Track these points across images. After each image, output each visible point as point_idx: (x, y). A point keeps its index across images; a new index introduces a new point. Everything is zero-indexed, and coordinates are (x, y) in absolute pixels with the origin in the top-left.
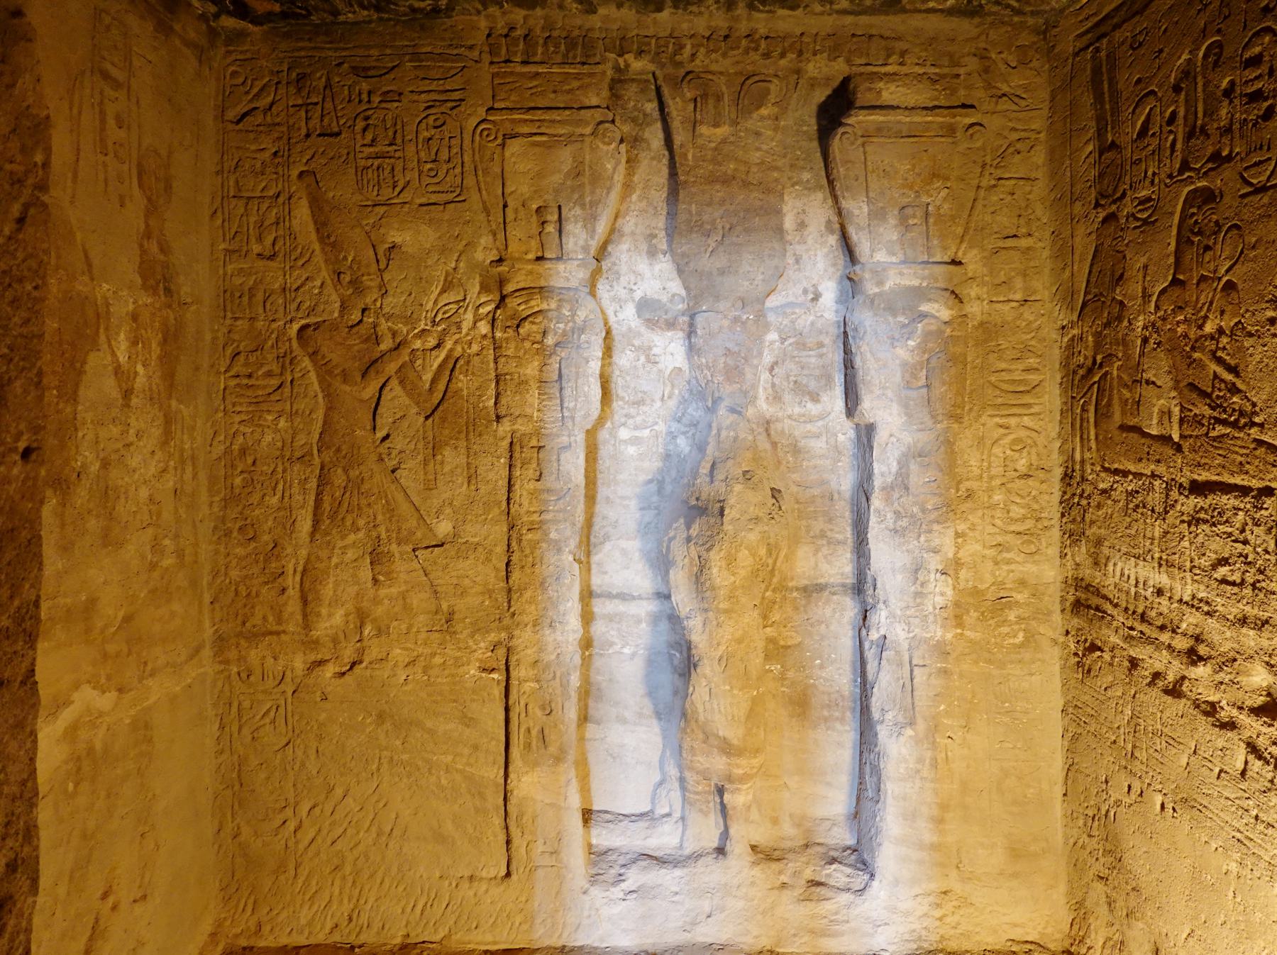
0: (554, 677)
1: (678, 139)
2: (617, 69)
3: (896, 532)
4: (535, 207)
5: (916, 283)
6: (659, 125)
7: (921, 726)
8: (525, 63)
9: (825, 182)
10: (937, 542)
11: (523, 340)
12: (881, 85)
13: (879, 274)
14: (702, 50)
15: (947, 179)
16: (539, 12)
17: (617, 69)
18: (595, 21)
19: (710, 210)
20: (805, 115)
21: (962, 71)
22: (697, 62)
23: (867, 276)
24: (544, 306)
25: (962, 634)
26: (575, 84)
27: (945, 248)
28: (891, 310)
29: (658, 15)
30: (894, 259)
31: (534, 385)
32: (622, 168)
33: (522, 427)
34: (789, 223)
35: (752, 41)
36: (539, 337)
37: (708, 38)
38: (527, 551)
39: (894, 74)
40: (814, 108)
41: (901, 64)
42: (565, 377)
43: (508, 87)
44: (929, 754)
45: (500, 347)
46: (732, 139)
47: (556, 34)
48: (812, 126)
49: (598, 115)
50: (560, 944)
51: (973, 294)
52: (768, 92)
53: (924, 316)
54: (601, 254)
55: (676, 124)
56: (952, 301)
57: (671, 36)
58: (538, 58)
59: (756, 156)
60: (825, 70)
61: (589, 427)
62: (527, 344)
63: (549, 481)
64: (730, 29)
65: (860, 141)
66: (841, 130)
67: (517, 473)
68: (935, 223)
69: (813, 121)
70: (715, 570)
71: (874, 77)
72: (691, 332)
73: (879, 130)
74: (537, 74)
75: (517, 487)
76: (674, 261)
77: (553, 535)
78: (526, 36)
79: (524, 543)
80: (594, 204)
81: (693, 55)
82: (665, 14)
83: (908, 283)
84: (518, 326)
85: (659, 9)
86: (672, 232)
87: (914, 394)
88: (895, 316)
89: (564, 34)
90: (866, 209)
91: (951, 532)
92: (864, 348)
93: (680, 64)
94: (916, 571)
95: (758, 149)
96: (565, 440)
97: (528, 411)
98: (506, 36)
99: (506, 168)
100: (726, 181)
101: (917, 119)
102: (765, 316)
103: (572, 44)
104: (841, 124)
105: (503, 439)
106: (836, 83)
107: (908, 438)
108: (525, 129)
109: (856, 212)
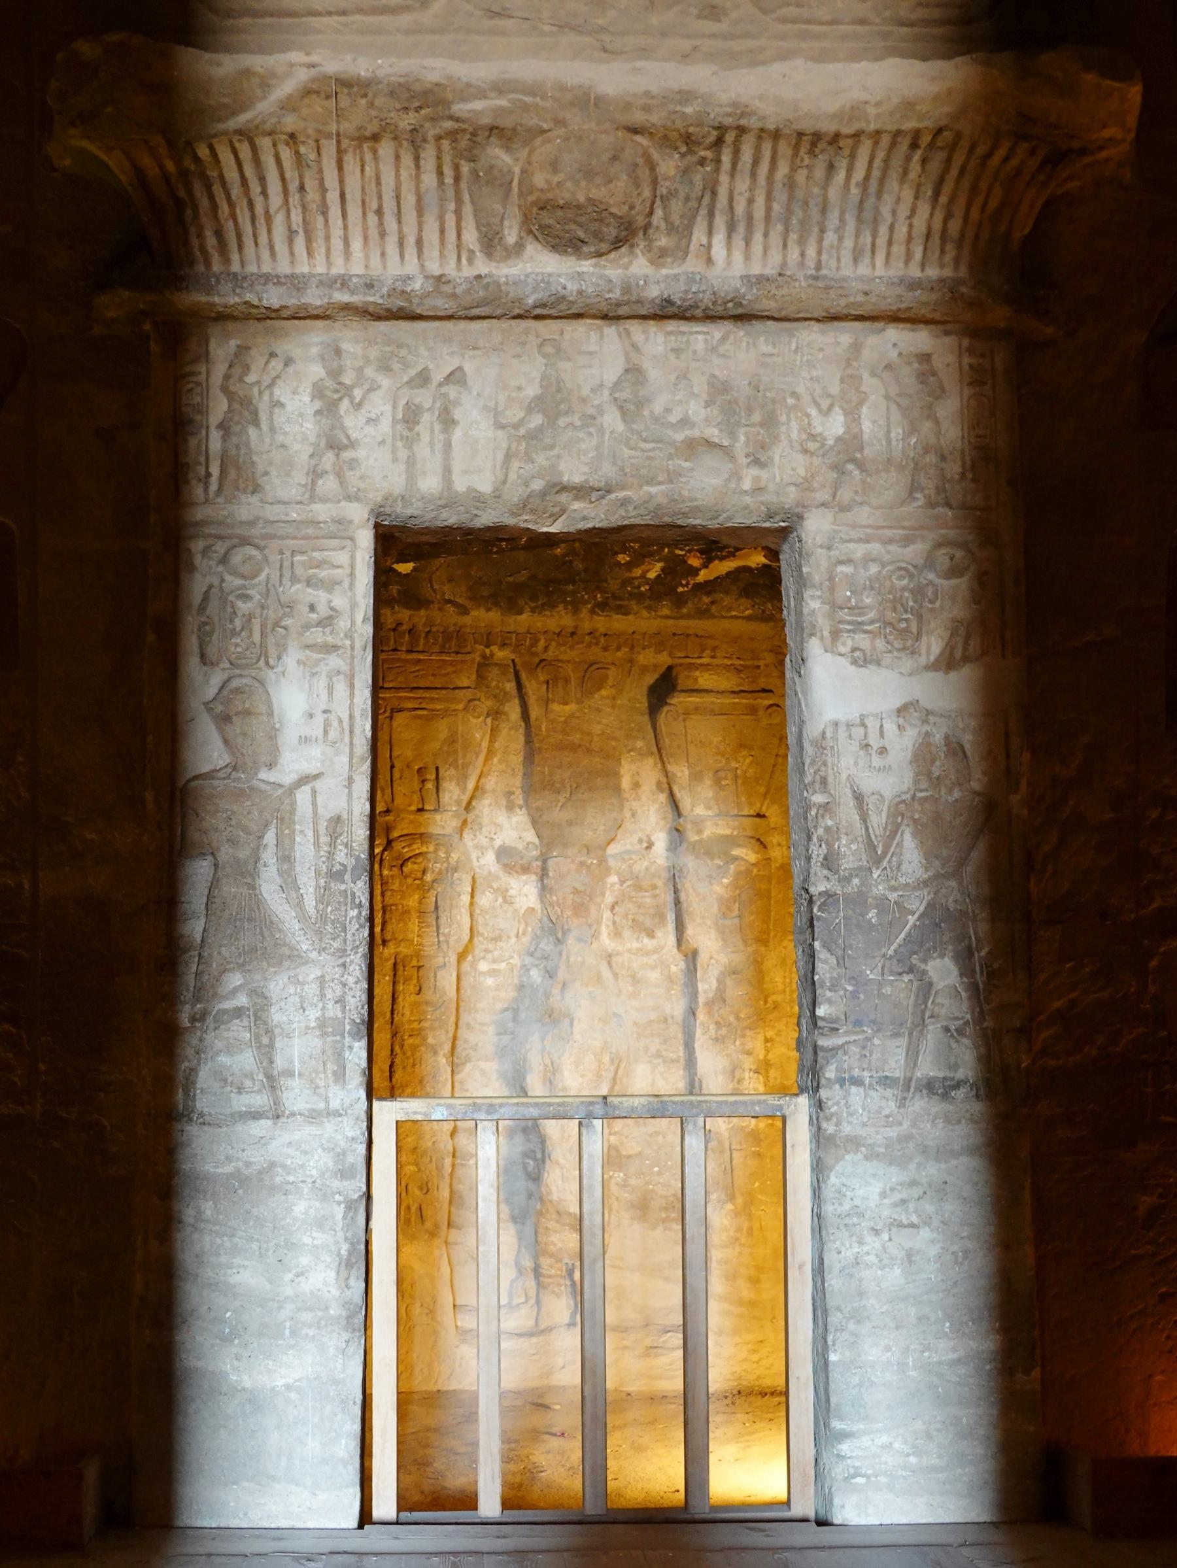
0: (431, 1161)
1: (535, 712)
2: (484, 656)
3: (717, 1040)
4: (416, 767)
5: (728, 832)
6: (517, 701)
7: (739, 1200)
8: (409, 651)
9: (655, 749)
10: (749, 1046)
11: (406, 877)
12: (697, 673)
13: (699, 825)
14: (554, 643)
15: (751, 748)
16: (423, 612)
17: (484, 656)
18: (467, 620)
19: (560, 771)
20: (637, 693)
21: (761, 663)
22: (550, 653)
23: (689, 826)
24: (424, 849)
25: (772, 1125)
26: (450, 669)
27: (751, 804)
28: (709, 854)
29: (518, 617)
30: (710, 813)
31: (414, 915)
32: (487, 737)
33: (404, 950)
34: (626, 783)
35: (595, 638)
36: (419, 875)
37: (558, 635)
38: (409, 1054)
39: (708, 665)
40: (645, 690)
41: (713, 657)
42: (441, 909)
43: (395, 671)
44: (746, 1225)
45: (387, 883)
46: (578, 714)
47: (434, 629)
48: (643, 703)
49: (469, 694)
50: (435, 1389)
51: (775, 841)
52: (607, 675)
53: (736, 858)
54: (468, 807)
55: (532, 700)
56: (757, 846)
57: (528, 632)
58: (420, 648)
59: (597, 729)
60: (654, 660)
61: (461, 950)
62: (409, 881)
63: (428, 994)
64: (576, 627)
65: (681, 718)
66: (666, 709)
67: (400, 987)
68: (743, 784)
69: (645, 700)
70: (566, 1073)
71: (691, 667)
72: (543, 874)
73: (697, 709)
74: (419, 661)
75: (400, 999)
76: (529, 814)
77: (430, 1040)
78: (410, 631)
79: (406, 1047)
80: (465, 766)
81: (546, 648)
82: (524, 616)
83: (722, 832)
84: (402, 865)
85: (520, 613)
86: (529, 790)
87: (728, 922)
88: (712, 859)
89: (442, 630)
90: (687, 772)
91: (761, 1037)
92: (688, 885)
93: (535, 654)
94: (733, 1071)
95: (600, 723)
96: (440, 960)
97: (410, 936)
98: (394, 630)
99: (394, 736)
100: (574, 748)
101: (727, 701)
102: (606, 861)
103: (447, 635)
104: (666, 703)
105: (387, 960)
106: (663, 669)
107: (724, 959)
108: (410, 705)
109: (679, 774)
